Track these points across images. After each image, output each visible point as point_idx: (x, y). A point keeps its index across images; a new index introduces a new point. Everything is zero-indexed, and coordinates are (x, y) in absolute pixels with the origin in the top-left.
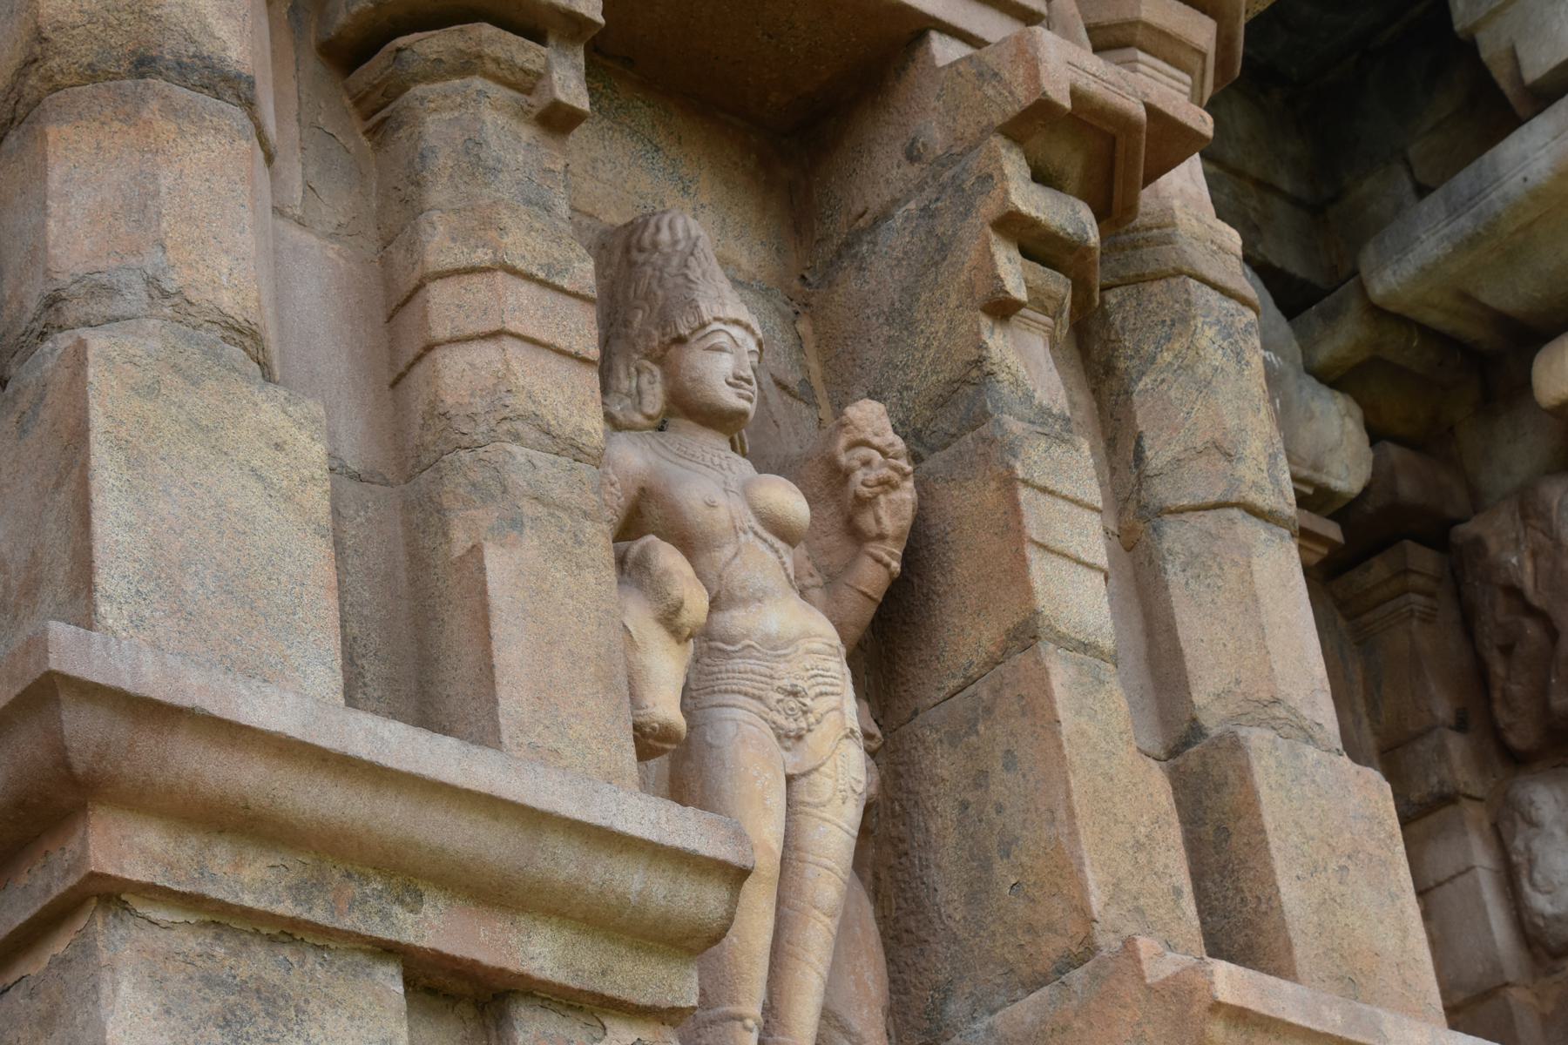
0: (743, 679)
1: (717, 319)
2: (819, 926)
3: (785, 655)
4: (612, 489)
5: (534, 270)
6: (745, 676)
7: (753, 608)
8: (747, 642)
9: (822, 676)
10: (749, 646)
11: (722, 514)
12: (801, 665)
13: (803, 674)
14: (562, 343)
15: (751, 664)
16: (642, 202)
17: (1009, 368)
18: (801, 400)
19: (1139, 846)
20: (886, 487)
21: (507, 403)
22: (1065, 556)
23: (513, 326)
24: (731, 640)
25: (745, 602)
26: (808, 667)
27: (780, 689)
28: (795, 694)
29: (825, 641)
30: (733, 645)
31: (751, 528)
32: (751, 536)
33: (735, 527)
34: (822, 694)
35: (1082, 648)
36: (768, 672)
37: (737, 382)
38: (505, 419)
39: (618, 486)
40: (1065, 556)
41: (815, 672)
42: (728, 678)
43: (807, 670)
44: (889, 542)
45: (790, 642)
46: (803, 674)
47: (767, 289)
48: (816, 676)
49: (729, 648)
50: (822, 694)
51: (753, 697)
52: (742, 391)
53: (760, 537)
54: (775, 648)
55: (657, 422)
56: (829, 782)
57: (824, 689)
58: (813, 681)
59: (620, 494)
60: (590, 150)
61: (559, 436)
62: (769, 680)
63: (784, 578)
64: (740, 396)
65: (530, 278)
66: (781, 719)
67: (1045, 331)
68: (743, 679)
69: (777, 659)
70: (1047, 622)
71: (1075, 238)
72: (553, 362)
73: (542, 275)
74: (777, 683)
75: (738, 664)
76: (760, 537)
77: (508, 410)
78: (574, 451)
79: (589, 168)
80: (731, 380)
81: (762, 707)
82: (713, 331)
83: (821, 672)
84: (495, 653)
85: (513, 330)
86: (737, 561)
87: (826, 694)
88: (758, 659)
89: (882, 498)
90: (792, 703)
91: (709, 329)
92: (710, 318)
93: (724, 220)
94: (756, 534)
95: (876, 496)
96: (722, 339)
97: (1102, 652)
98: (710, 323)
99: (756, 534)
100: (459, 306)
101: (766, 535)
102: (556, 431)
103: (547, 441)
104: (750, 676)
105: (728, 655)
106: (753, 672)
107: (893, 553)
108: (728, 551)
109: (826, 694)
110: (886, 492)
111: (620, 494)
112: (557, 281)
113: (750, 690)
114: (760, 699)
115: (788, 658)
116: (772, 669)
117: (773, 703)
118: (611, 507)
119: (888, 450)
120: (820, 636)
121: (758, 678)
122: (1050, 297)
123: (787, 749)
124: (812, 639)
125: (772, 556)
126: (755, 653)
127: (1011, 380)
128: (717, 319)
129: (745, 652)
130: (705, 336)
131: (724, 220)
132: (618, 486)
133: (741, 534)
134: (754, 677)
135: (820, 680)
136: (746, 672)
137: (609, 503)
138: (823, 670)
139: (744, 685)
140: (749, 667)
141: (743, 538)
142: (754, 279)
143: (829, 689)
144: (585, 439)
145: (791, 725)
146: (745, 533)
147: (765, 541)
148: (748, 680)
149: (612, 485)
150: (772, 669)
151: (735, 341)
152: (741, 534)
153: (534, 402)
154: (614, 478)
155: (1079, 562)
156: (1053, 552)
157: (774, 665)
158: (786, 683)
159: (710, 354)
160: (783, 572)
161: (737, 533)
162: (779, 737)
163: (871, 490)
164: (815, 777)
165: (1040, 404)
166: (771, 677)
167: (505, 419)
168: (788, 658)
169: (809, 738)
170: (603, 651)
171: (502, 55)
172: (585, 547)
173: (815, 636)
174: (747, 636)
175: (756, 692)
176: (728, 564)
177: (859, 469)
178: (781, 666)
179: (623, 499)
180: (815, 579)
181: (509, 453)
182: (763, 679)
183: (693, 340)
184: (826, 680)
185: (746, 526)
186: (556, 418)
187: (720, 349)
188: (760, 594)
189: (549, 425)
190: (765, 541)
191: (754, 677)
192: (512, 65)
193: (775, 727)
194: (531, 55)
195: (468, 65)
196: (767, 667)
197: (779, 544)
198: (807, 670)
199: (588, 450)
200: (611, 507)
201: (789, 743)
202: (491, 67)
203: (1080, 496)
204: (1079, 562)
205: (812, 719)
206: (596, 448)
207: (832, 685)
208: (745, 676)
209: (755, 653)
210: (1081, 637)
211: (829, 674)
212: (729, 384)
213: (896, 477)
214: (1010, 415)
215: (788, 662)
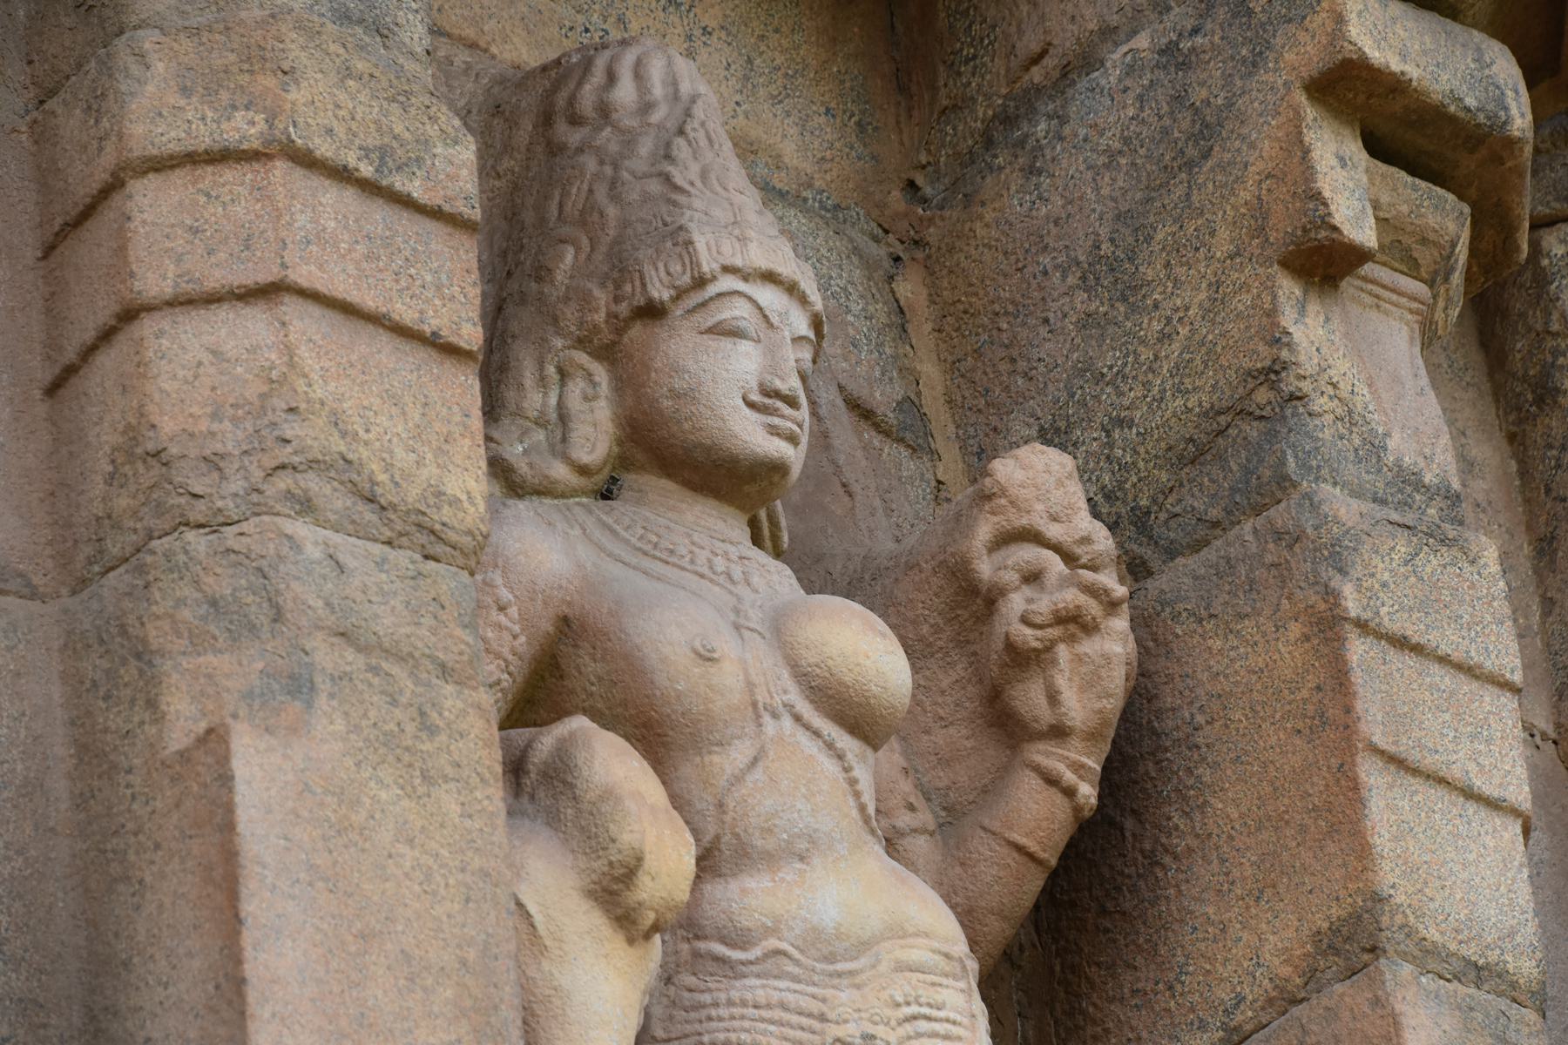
0: (763, 1020)
1: (727, 269)
3: (851, 973)
4: (502, 618)
5: (351, 159)
6: (765, 1013)
7: (788, 873)
8: (773, 943)
9: (929, 1018)
11: (729, 677)
12: (885, 995)
13: (888, 1012)
14: (405, 313)
16: (580, 18)
17: (1335, 386)
18: (901, 440)
20: (1072, 628)
21: (289, 434)
22: (1442, 781)
23: (303, 275)
24: (741, 940)
25: (770, 860)
26: (900, 999)
29: (936, 945)
30: (743, 949)
31: (789, 707)
32: (787, 722)
33: (754, 704)
35: (1472, 975)
36: (815, 1006)
37: (767, 401)
38: (283, 467)
39: (513, 611)
40: (1442, 781)
41: (914, 1009)
42: (733, 1018)
43: (898, 1005)
44: (1075, 742)
45: (864, 946)
46: (888, 1012)
47: (837, 207)
48: (915, 1018)
49: (736, 955)
52: (776, 421)
53: (807, 727)
54: (830, 958)
55: (600, 479)
58: (909, 1028)
59: (517, 628)
61: (394, 507)
62: (816, 1025)
63: (855, 813)
64: (774, 431)
65: (341, 175)
67: (1411, 311)
68: (763, 1020)
69: (836, 981)
70: (1399, 919)
71: (1481, 118)
72: (382, 349)
73: (366, 170)
75: (755, 988)
76: (807, 727)
77: (289, 449)
78: (423, 538)
80: (755, 397)
82: (720, 295)
83: (925, 1010)
84: (248, 953)
85: (304, 282)
86: (758, 774)
88: (796, 979)
89: (1062, 651)
91: (712, 290)
92: (715, 266)
93: (750, 61)
94: (798, 718)
95: (1050, 648)
96: (738, 311)
97: (1514, 985)
98: (714, 278)
99: (798, 718)
100: (195, 231)
101: (818, 721)
102: (387, 495)
103: (368, 515)
104: (777, 1014)
106: (784, 1006)
107: (1083, 766)
108: (739, 754)
110: (1071, 639)
111: (517, 628)
112: (399, 183)
115: (857, 980)
116: (824, 1000)
118: (498, 656)
119: (1078, 550)
120: (927, 935)
121: (795, 1019)
122: (1424, 241)
124: (911, 941)
125: (829, 766)
126: (790, 968)
127: (1339, 411)
128: (727, 269)
129: (769, 965)
130: (704, 304)
131: (750, 61)
132: (513, 611)
133: (767, 719)
134: (786, 1016)
135: (923, 1026)
136: (769, 1006)
137: (494, 645)
138: (930, 1005)
139: (764, 1033)
140: (776, 996)
142: (810, 186)
144: (446, 513)
146: (775, 716)
147: (817, 734)
148: (772, 1022)
149: (502, 609)
150: (824, 1000)
151: (765, 316)
152: (767, 719)
153: (344, 434)
154: (505, 595)
155: (1470, 794)
156: (1415, 772)
157: (828, 993)
159: (711, 342)
160: (851, 802)
161: (758, 716)
163: (1039, 633)
165: (1398, 461)
166: (822, 1018)
167: (283, 467)
168: (857, 980)
170: (472, 955)
172: (443, 737)
173: (916, 935)
174: (773, 931)
176: (738, 779)
177: (1017, 589)
178: (844, 996)
179: (523, 639)
180: (920, 815)
181: (289, 537)
182: (805, 1021)
183: (678, 313)
184: (937, 1027)
185: (777, 701)
186: (388, 467)
187: (733, 332)
188: (802, 845)
189: (373, 483)
190: (817, 734)
191: (786, 1016)
196: (814, 997)
197: (845, 741)
198: (898, 1005)
199: (451, 536)
200: (498, 656)
203: (1476, 658)
204: (1470, 794)
206: (469, 533)
208: (765, 1013)
209: (790, 968)
210: (1470, 951)
211: (942, 1014)
212: (751, 405)
213: (1093, 608)
214: (1335, 484)
215: (858, 987)
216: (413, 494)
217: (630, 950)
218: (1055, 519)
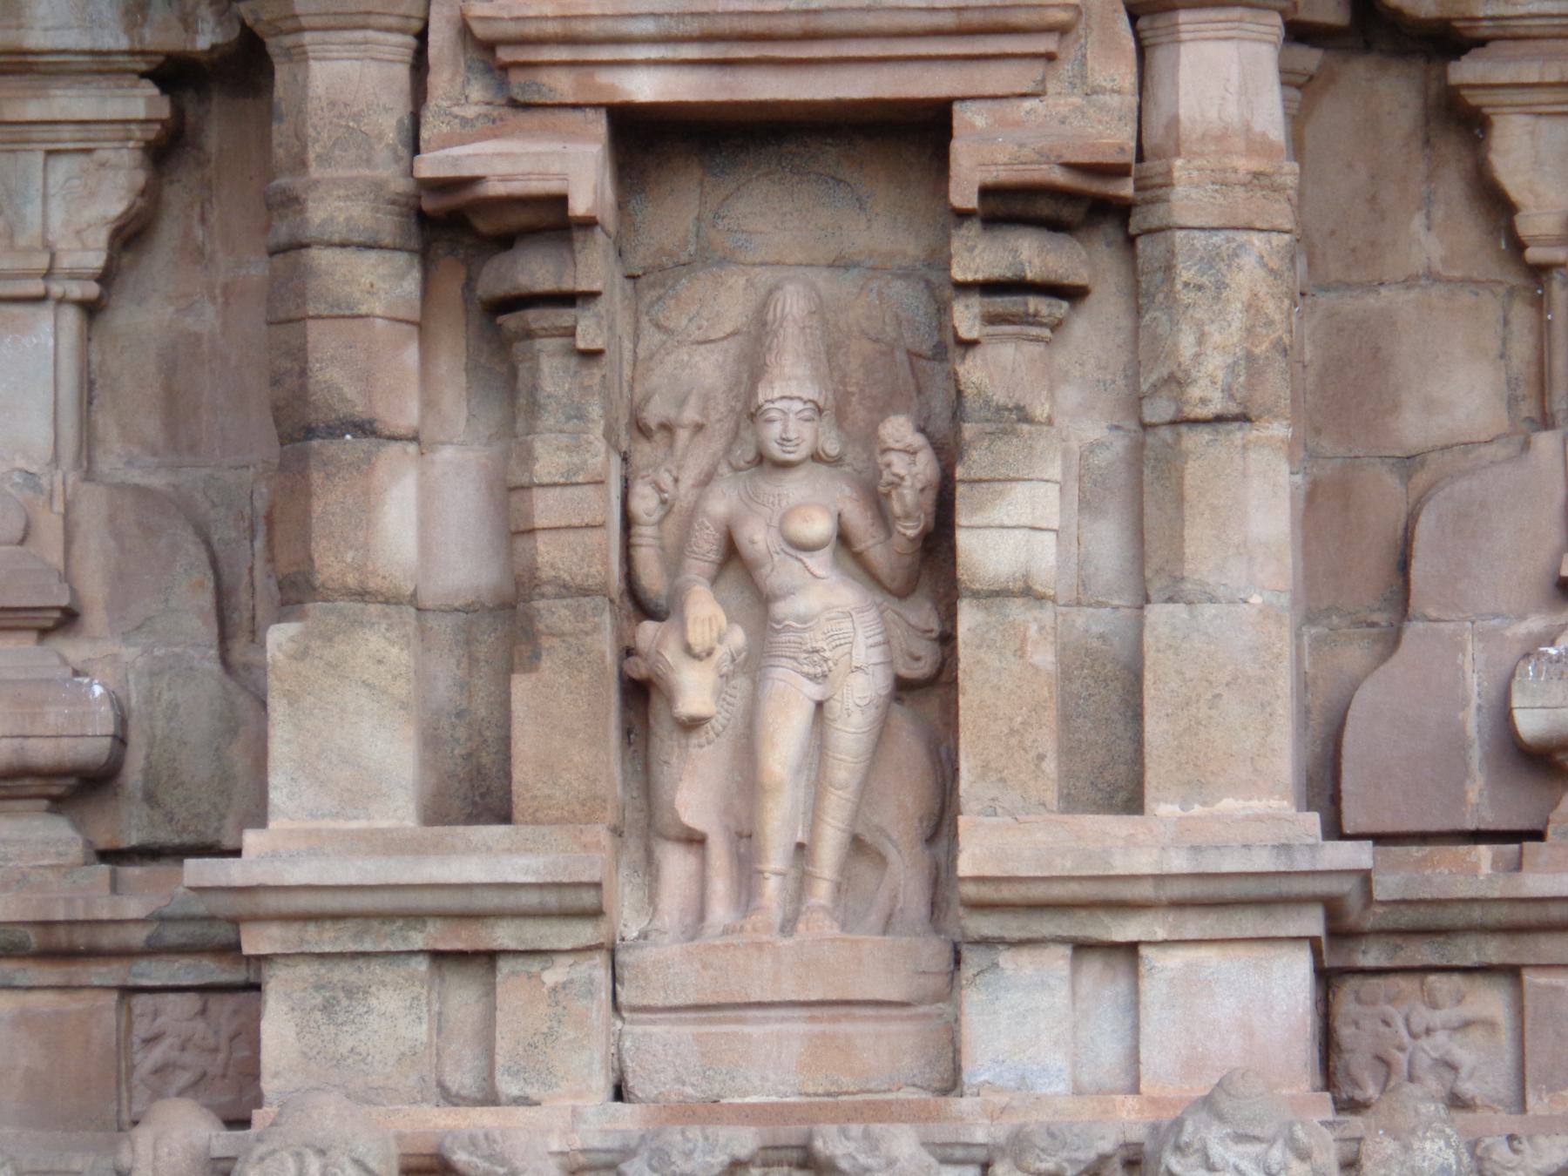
1: (767, 401)
2: (832, 797)
4: (708, 531)
8: (787, 622)
10: (787, 626)
13: (824, 637)
15: (791, 637)
19: (1012, 732)
24: (778, 622)
25: (783, 597)
27: (807, 652)
28: (817, 651)
29: (840, 609)
31: (782, 550)
32: (783, 555)
34: (837, 646)
36: (799, 640)
50: (837, 646)
51: (790, 658)
52: (784, 448)
54: (805, 623)
56: (839, 705)
57: (838, 642)
60: (781, 207)
64: (784, 451)
65: (555, 485)
66: (811, 670)
73: (562, 480)
74: (804, 648)
75: (783, 637)
79: (778, 224)
81: (795, 664)
86: (775, 573)
87: (841, 645)
89: (894, 494)
90: (816, 657)
96: (773, 414)
97: (1013, 592)
101: (794, 552)
103: (564, 591)
105: (778, 632)
109: (841, 645)
112: (574, 480)
113: (788, 654)
114: (795, 659)
117: (801, 661)
120: (837, 607)
123: (819, 684)
125: (798, 564)
128: (767, 401)
130: (762, 414)
132: (712, 529)
135: (836, 637)
141: (776, 558)
143: (842, 641)
144: (590, 581)
145: (819, 670)
146: (778, 553)
147: (791, 556)
149: (708, 528)
152: (775, 556)
155: (1002, 527)
158: (809, 647)
162: (810, 679)
164: (832, 701)
169: (830, 675)
171: (546, 325)
175: (792, 655)
176: (768, 576)
178: (807, 635)
185: (778, 550)
186: (570, 575)
187: (771, 421)
189: (564, 580)
192: (556, 328)
193: (807, 676)
194: (566, 317)
195: (529, 335)
197: (802, 555)
201: (820, 681)
202: (544, 332)
204: (1002, 527)
205: (831, 663)
207: (844, 638)
213: (896, 480)
216: (578, 580)
217: (703, 663)
218: (897, 441)
